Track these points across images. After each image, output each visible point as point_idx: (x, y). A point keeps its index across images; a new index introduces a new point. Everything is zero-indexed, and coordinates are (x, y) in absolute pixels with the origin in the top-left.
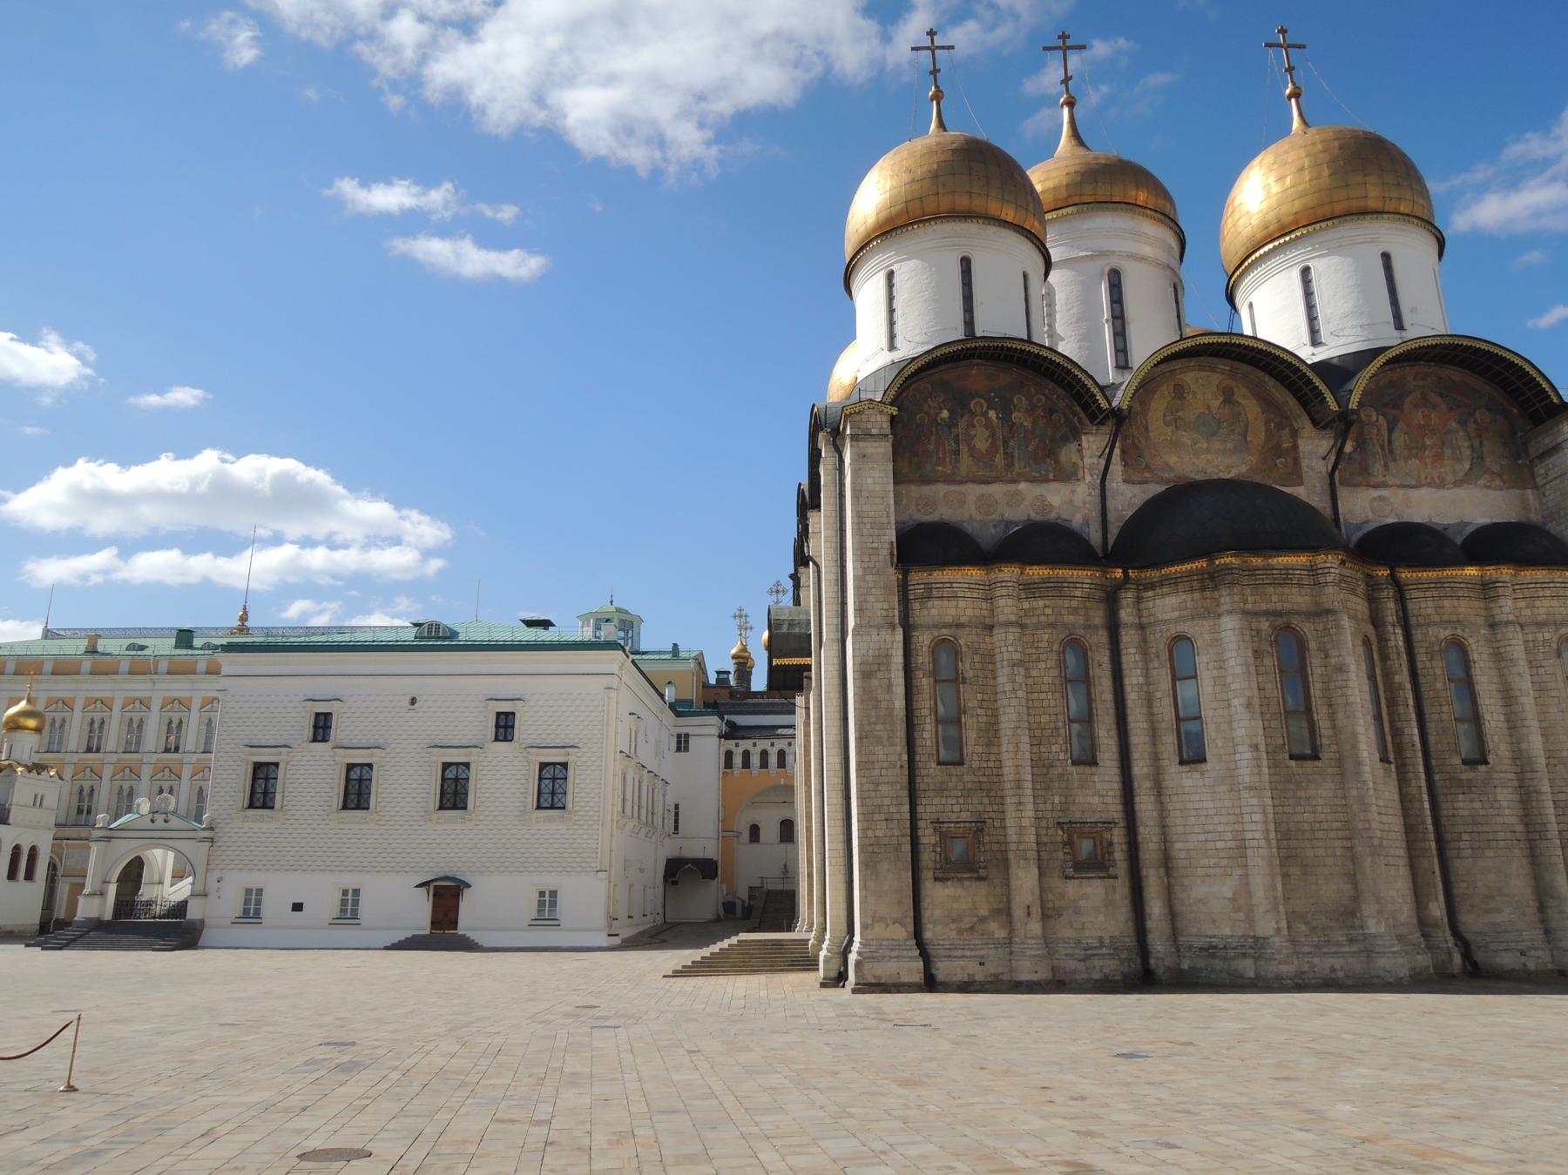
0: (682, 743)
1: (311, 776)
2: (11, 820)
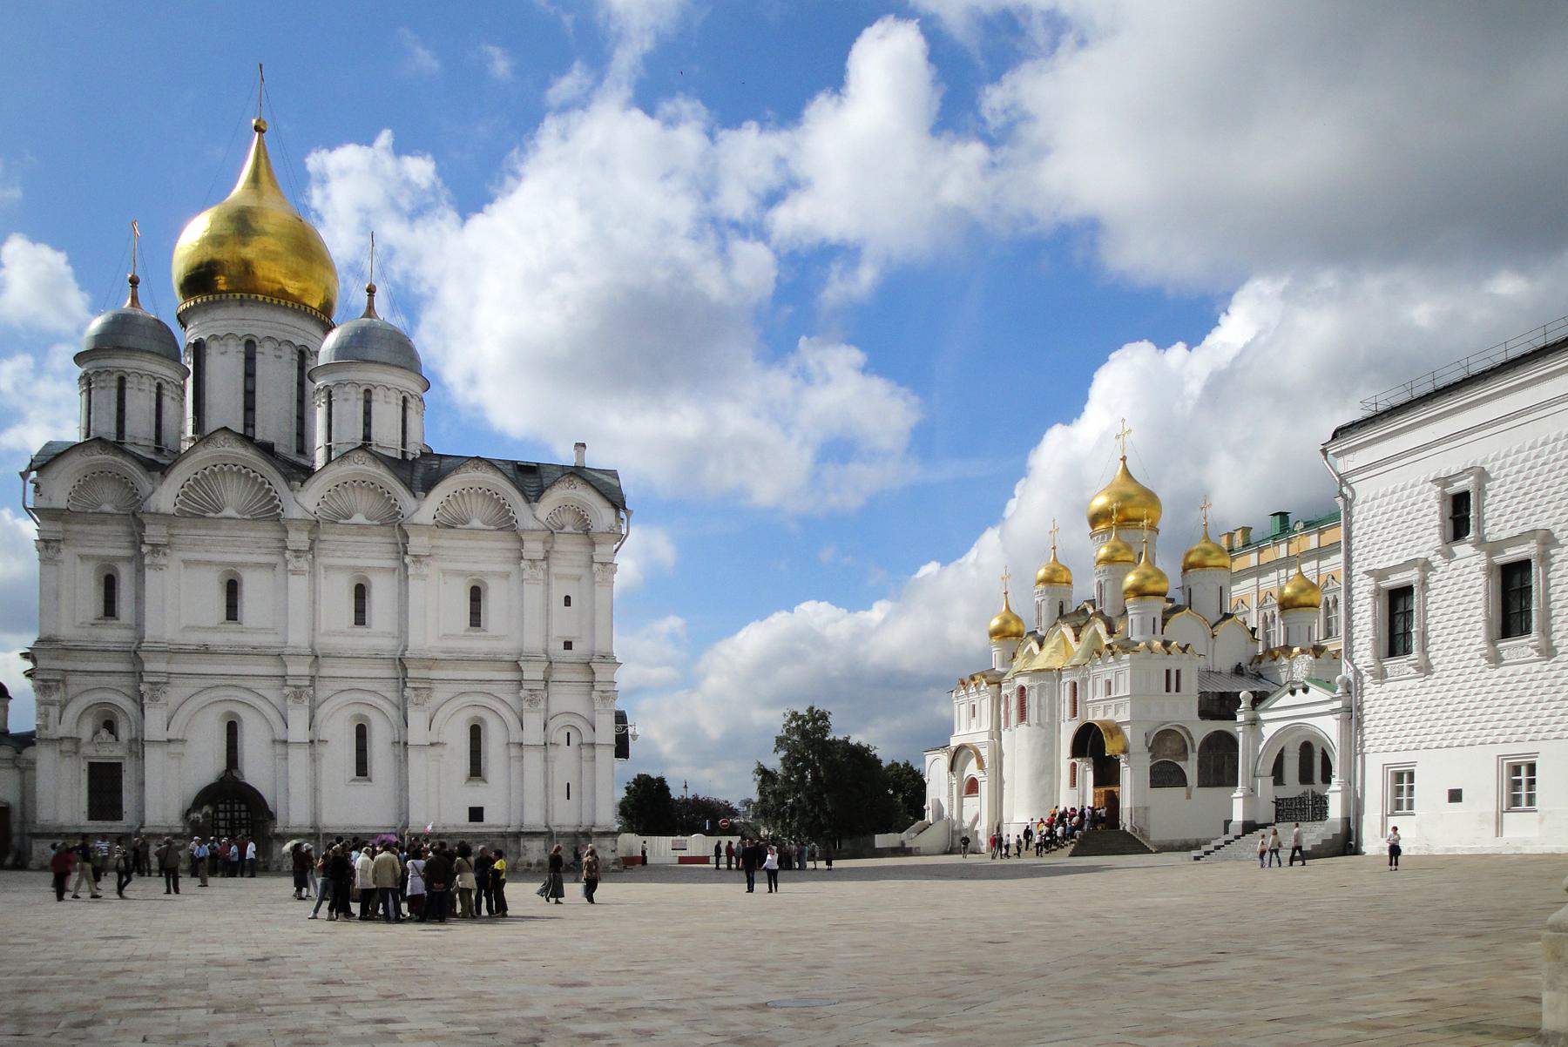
1: (1458, 598)
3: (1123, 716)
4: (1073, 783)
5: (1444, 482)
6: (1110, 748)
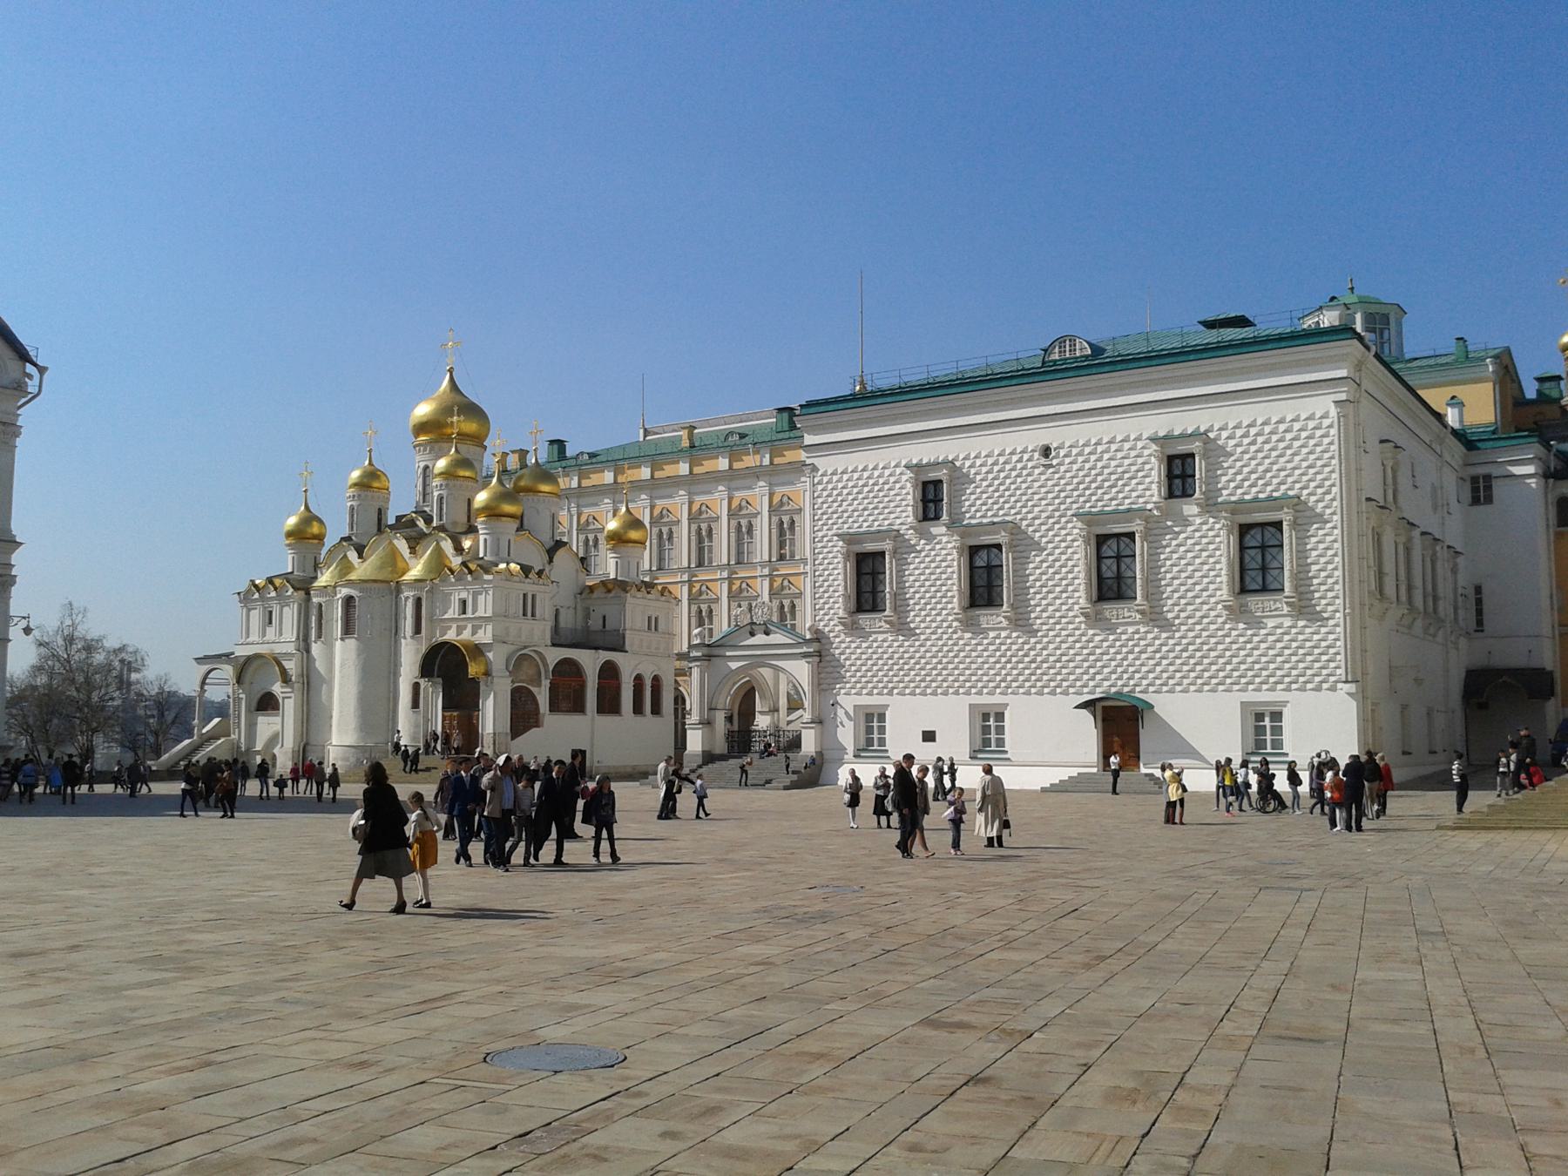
0: (1481, 491)
2: (627, 647)
3: (484, 636)
4: (415, 704)
5: (917, 468)
6: (473, 670)
